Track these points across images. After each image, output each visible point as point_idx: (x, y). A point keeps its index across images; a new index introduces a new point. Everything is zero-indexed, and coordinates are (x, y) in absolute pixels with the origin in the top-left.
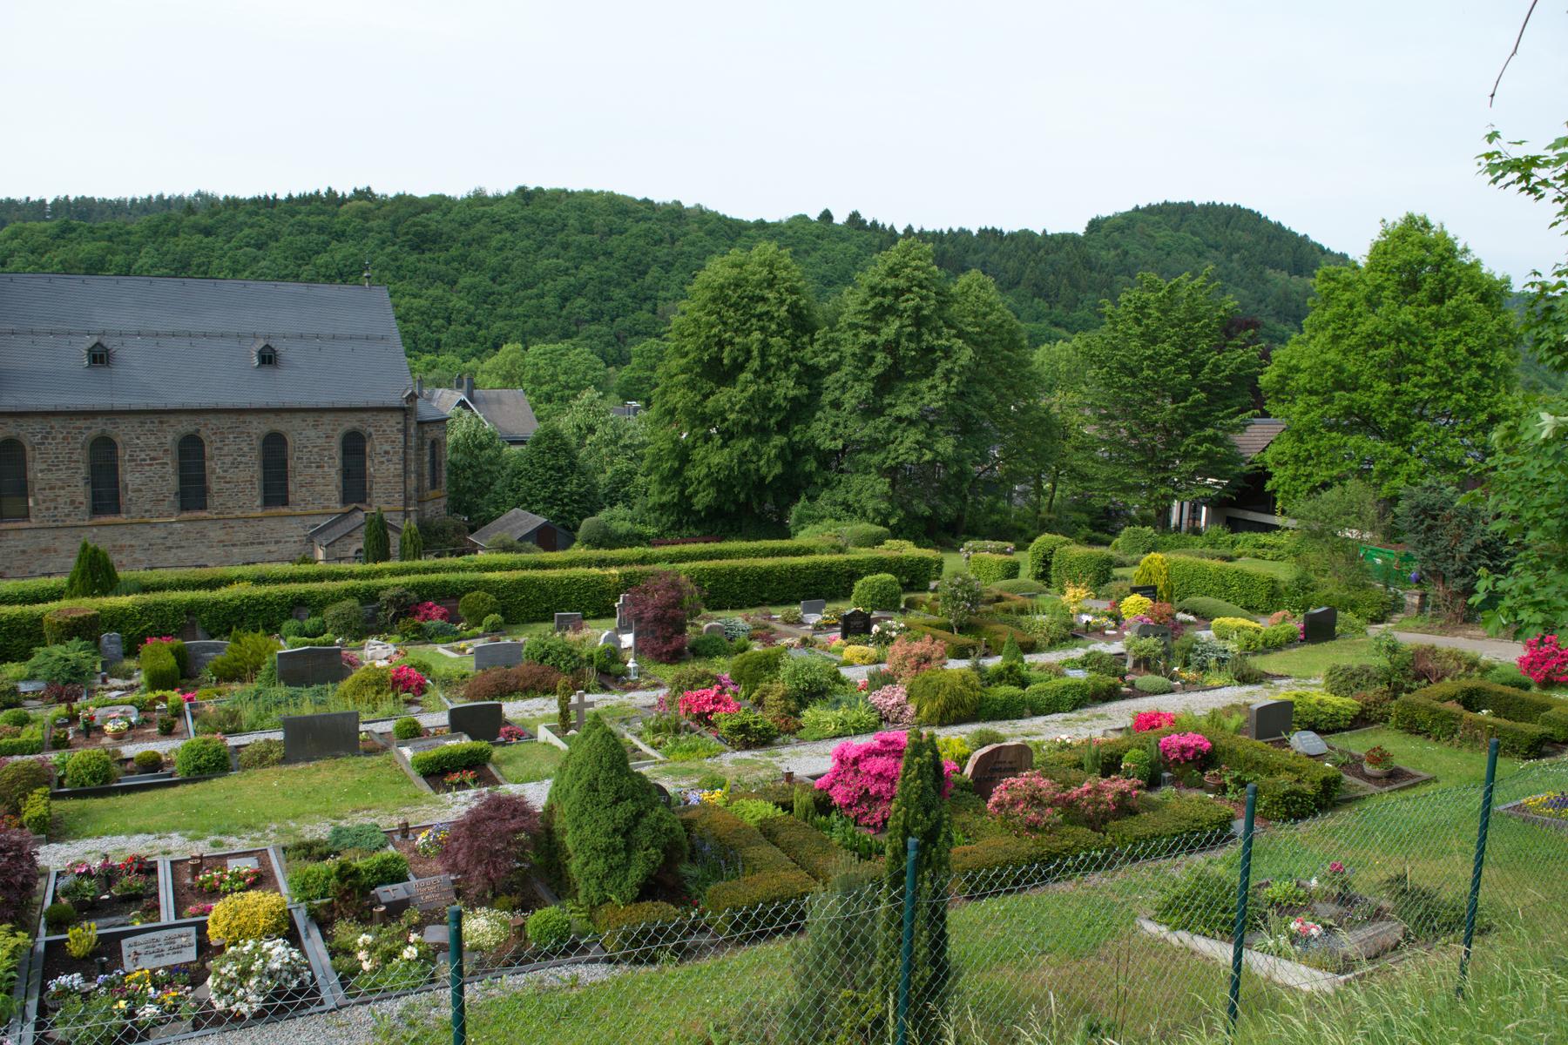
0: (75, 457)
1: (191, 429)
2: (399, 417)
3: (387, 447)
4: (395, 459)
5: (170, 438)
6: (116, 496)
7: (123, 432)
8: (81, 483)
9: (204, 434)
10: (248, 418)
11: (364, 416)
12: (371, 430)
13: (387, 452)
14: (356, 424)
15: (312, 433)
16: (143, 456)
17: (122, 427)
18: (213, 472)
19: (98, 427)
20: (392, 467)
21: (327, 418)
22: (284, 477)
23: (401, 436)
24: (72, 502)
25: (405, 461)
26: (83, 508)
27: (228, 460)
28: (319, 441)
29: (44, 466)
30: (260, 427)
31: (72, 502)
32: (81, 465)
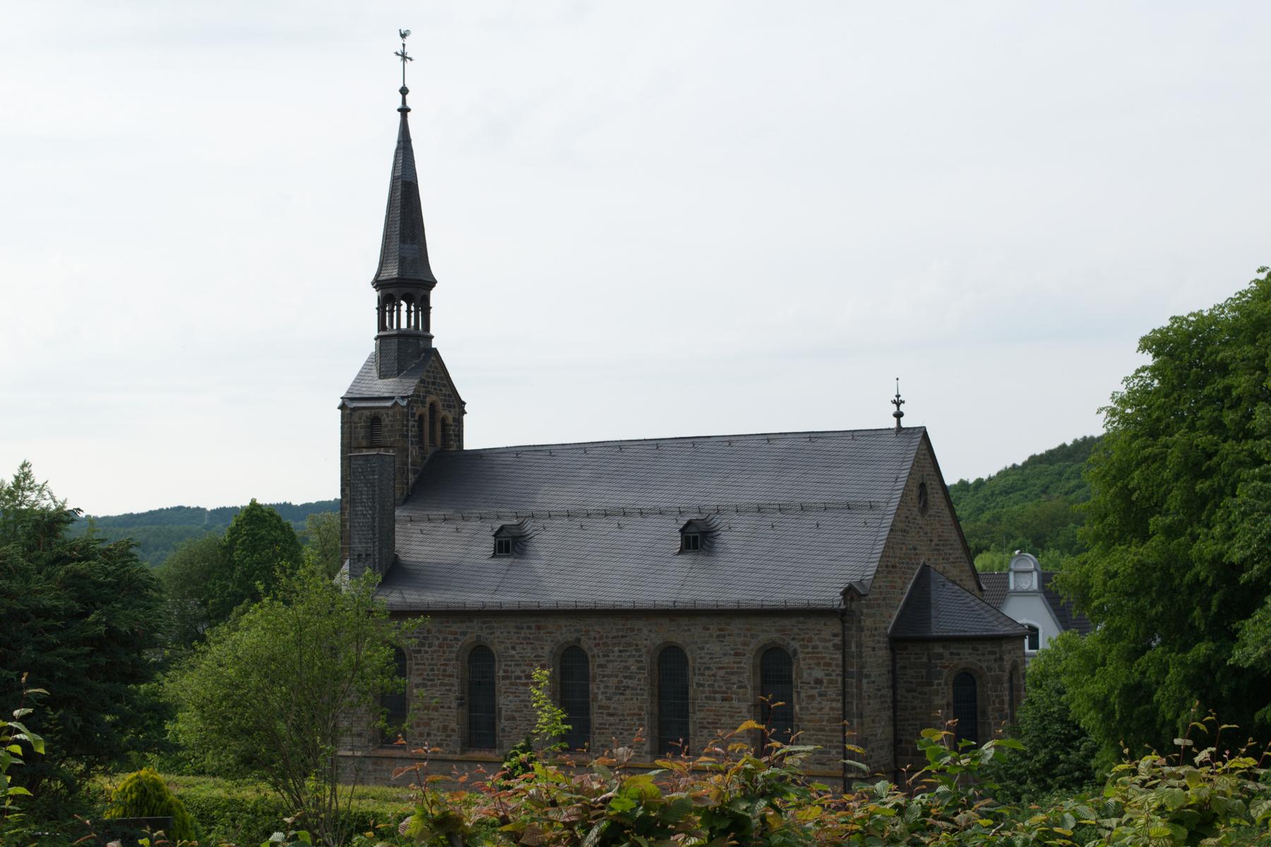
0: (450, 670)
1: (571, 637)
2: (834, 626)
3: (818, 673)
4: (832, 692)
5: (547, 649)
6: (492, 726)
7: (500, 639)
8: (454, 705)
9: (585, 644)
10: (639, 624)
11: (787, 623)
12: (795, 645)
13: (818, 681)
14: (774, 635)
15: (716, 648)
16: (518, 673)
17: (498, 633)
18: (595, 699)
19: (474, 631)
20: (827, 705)
21: (736, 626)
22: (684, 713)
23: (839, 656)
24: (445, 728)
25: (844, 694)
26: (455, 737)
27: (613, 682)
28: (726, 659)
29: (418, 680)
30: (651, 636)
31: (445, 728)
32: (455, 681)
